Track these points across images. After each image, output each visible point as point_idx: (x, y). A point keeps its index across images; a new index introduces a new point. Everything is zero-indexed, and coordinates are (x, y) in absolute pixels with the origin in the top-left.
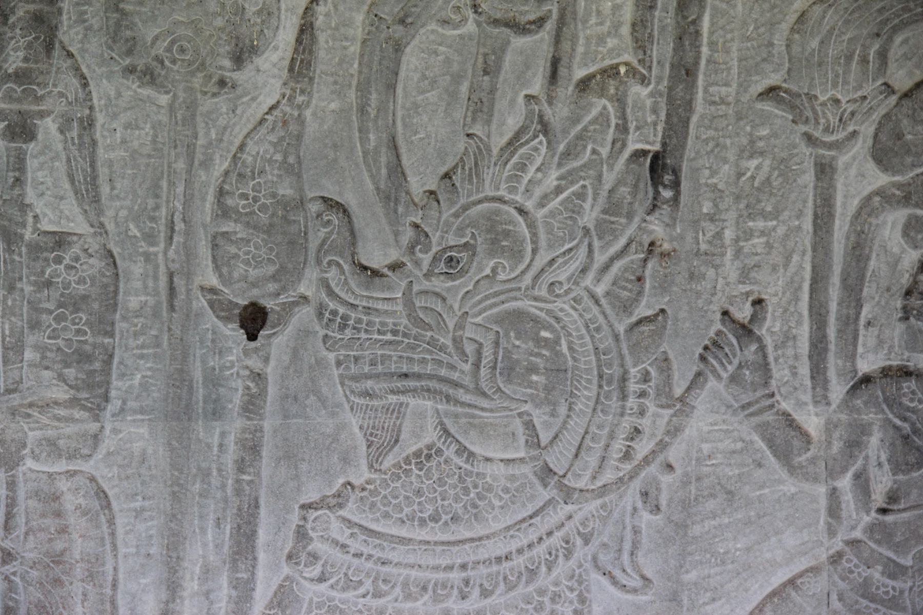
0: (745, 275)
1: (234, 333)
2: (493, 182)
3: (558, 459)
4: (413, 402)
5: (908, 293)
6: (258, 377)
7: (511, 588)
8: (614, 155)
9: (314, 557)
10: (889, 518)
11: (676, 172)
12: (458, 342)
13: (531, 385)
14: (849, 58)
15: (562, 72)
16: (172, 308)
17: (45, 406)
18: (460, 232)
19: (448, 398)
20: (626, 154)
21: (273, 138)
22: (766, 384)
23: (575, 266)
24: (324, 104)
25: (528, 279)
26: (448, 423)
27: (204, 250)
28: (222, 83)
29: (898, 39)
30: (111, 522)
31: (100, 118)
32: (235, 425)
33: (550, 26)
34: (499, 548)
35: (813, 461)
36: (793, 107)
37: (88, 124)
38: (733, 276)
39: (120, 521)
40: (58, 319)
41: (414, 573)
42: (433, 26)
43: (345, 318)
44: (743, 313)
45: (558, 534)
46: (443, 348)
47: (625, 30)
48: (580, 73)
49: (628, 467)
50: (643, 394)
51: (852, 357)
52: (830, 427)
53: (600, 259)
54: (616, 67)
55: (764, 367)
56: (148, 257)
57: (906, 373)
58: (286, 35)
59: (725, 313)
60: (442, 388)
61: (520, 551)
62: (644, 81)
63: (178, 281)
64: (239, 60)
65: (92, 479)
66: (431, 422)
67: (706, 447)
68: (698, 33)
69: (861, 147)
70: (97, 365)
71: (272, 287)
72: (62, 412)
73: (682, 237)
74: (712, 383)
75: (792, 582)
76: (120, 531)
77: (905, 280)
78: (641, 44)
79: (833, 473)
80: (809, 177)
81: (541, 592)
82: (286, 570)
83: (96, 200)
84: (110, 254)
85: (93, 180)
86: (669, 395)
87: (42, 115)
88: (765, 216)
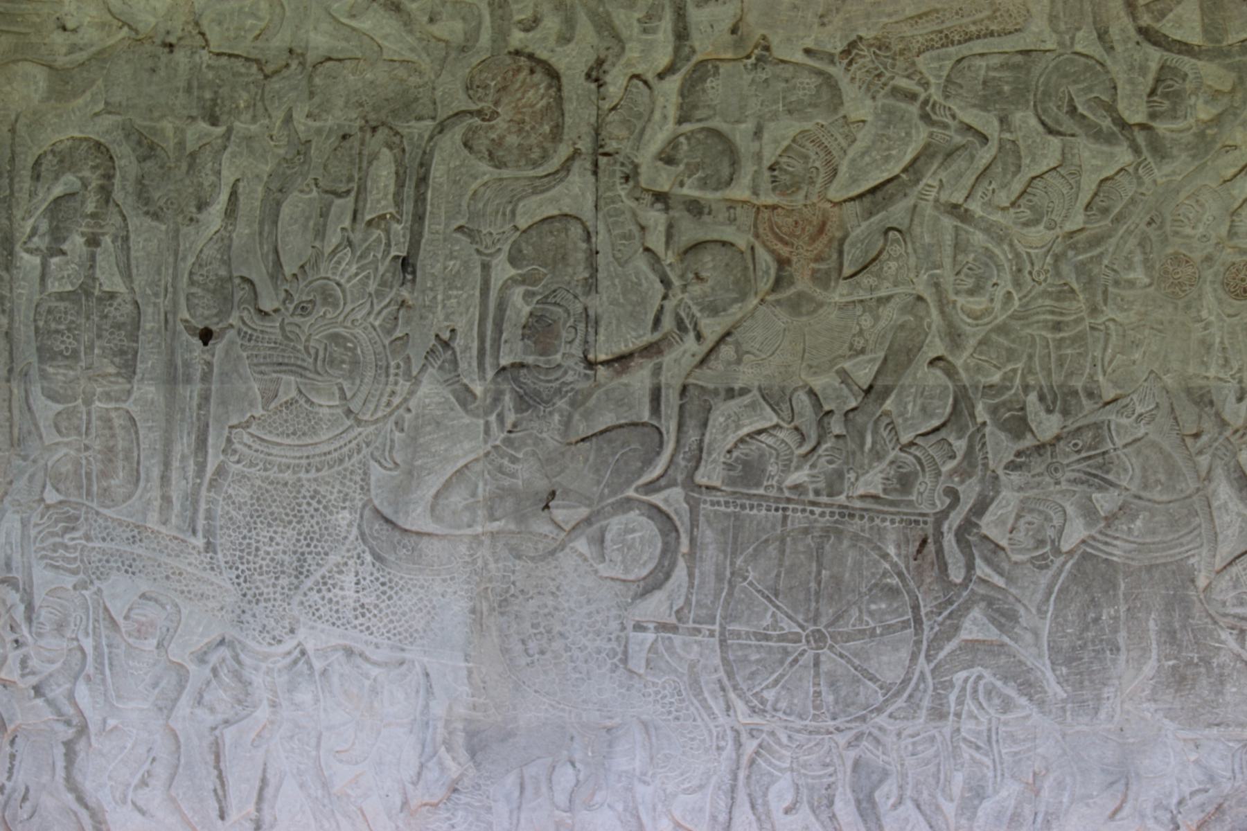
0: (447, 318)
1: (196, 342)
2: (325, 269)
3: (355, 406)
4: (285, 377)
5: (524, 327)
6: (209, 364)
7: (331, 467)
8: (384, 258)
9: (235, 451)
10: (513, 435)
11: (414, 266)
12: (306, 348)
13: (342, 369)
14: (497, 212)
15: (359, 216)
16: (166, 329)
17: (104, 376)
18: (308, 294)
19: (301, 375)
20: (390, 258)
21: (216, 247)
22: (456, 370)
23: (364, 311)
24: (242, 231)
25: (341, 318)
26: (302, 387)
27: (183, 301)
28: (191, 219)
29: (521, 205)
30: (137, 432)
31: (132, 236)
32: (198, 387)
33: (353, 194)
34: (325, 448)
35: (477, 408)
36: (470, 236)
37: (126, 239)
38: (442, 317)
39: (141, 432)
40: (112, 333)
41: (284, 460)
42: (296, 193)
43: (251, 335)
44: (446, 336)
45: (354, 442)
46: (299, 351)
47: (390, 197)
48: (368, 217)
49: (389, 410)
50: (396, 375)
51: (497, 358)
52: (486, 391)
53: (377, 308)
54: (385, 215)
55: (455, 362)
56: (155, 304)
57: (522, 365)
58: (224, 197)
59: (437, 336)
60: (299, 371)
61: (335, 450)
62: (399, 222)
63: (170, 317)
64: (200, 208)
65: (128, 412)
66: (293, 387)
67: (427, 401)
68: (425, 200)
69: (503, 256)
70: (130, 356)
71: (216, 320)
72: (113, 379)
73: (417, 299)
74: (430, 370)
75: (466, 466)
76: (141, 437)
77: (523, 321)
78: (398, 202)
79: (487, 413)
80: (478, 270)
81: (345, 470)
82: (222, 457)
83: (130, 276)
84: (136, 302)
85: (129, 266)
86: (410, 375)
87: (103, 234)
88: (457, 288)
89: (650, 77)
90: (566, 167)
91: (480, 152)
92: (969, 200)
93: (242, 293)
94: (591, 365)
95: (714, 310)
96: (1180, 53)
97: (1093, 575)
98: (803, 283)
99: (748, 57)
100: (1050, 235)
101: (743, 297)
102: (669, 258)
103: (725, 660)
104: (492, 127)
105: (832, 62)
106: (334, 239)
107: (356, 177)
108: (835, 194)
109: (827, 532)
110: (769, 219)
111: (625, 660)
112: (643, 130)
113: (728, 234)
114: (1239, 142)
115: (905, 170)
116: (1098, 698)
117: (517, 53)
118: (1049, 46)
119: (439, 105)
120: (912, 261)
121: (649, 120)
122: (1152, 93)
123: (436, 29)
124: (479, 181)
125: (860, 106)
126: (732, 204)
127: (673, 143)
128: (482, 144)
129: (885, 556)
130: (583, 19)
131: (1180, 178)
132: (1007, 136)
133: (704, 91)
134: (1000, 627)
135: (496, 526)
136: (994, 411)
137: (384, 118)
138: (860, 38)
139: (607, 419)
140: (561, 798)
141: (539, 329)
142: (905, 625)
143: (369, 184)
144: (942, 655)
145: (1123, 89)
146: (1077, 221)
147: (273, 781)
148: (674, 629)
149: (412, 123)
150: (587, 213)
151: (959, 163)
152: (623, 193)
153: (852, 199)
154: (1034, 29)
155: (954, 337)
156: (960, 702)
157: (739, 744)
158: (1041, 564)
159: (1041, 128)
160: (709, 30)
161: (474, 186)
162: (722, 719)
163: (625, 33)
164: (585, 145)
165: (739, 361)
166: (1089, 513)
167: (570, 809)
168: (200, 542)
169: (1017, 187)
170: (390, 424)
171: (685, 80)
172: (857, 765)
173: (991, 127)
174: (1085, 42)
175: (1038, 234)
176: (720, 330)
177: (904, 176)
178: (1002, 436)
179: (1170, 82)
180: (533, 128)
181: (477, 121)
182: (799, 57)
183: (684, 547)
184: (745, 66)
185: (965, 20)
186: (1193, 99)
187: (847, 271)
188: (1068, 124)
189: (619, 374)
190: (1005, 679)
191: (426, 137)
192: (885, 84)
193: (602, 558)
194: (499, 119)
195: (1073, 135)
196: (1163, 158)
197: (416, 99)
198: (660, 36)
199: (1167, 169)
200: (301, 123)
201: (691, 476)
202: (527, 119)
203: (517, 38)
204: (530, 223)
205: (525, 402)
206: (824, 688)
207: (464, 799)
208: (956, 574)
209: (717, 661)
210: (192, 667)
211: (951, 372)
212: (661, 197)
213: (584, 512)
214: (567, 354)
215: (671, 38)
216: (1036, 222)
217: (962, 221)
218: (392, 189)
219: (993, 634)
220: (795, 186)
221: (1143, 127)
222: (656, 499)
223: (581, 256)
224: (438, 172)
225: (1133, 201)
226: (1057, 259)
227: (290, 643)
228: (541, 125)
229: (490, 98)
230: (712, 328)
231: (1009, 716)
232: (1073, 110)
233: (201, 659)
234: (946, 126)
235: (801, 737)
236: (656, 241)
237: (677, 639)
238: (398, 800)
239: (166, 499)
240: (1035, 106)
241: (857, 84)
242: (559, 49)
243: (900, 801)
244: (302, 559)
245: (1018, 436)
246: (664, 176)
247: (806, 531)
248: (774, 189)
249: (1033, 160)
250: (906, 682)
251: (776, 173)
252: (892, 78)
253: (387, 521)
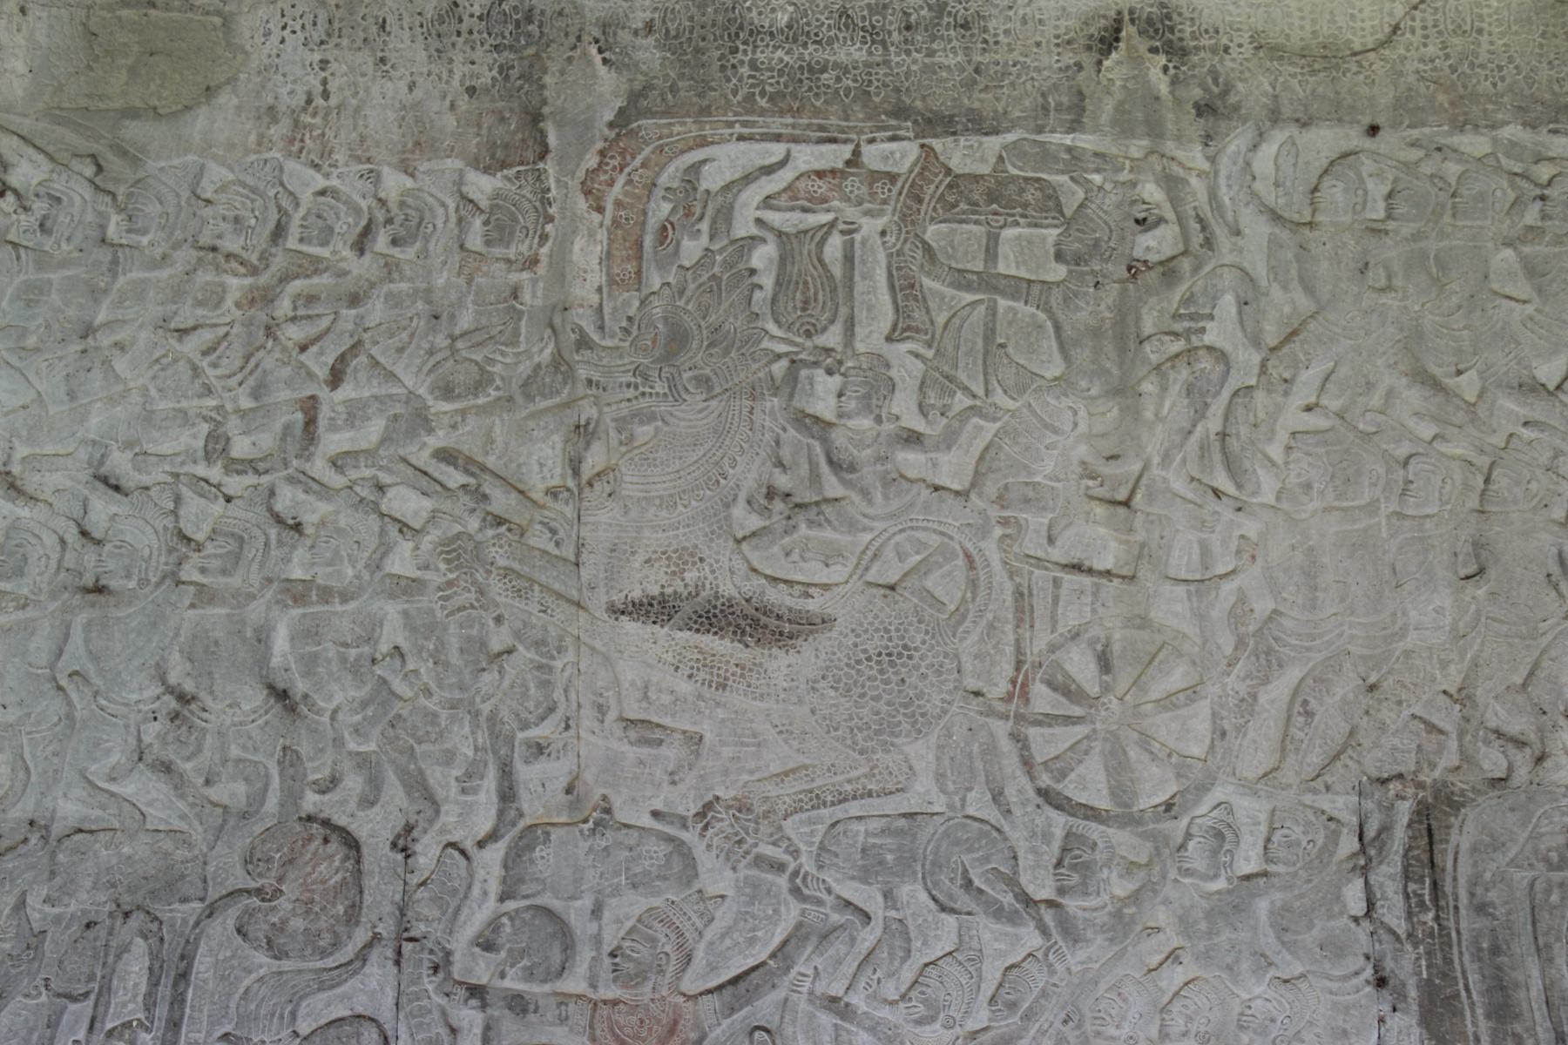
14: (273, 1015)
15: (97, 1025)
29: (304, 1004)
33: (93, 997)
42: (20, 998)
47: (140, 999)
48: (109, 1026)
54: (131, 1022)
62: (148, 1030)
68: (183, 1001)
78: (149, 1006)
89: (469, 845)
90: (362, 957)
91: (257, 939)
92: (851, 992)
96: (1086, 818)
99: (585, 821)
104: (273, 909)
105: (685, 827)
107: (99, 975)
108: (690, 984)
110: (609, 1018)
112: (458, 910)
114: (1162, 924)
115: (773, 956)
117: (310, 819)
118: (936, 809)
119: (210, 883)
121: (466, 897)
122: (1059, 864)
123: (213, 793)
124: (254, 976)
125: (717, 877)
126: (563, 999)
127: (494, 925)
128: (259, 929)
130: (391, 777)
131: (1097, 966)
132: (893, 914)
133: (532, 861)
137: (134, 906)
138: (717, 798)
143: (115, 982)
145: (1025, 860)
146: (981, 1018)
149: (176, 906)
150: (386, 1014)
151: (838, 947)
152: (430, 988)
153: (710, 992)
154: (919, 787)
159: (932, 905)
160: (540, 789)
161: (246, 983)
163: (440, 794)
164: (386, 929)
169: (908, 975)
171: (509, 847)
174: (978, 803)
177: (771, 962)
179: (1077, 852)
180: (323, 909)
181: (255, 901)
182: (647, 821)
184: (581, 831)
185: (840, 778)
186: (1106, 871)
188: (964, 901)
191: (191, 923)
192: (747, 853)
194: (282, 899)
195: (969, 914)
196: (1076, 941)
197: (183, 877)
198: (482, 797)
199: (1081, 955)
200: (36, 909)
202: (317, 898)
203: (311, 801)
204: (314, 1026)
212: (476, 992)
215: (495, 799)
216: (930, 1019)
217: (842, 1019)
218: (143, 989)
220: (639, 977)
221: (1050, 903)
224: (203, 966)
225: (1044, 994)
228: (334, 904)
229: (273, 874)
232: (968, 884)
234: (820, 902)
240: (924, 878)
241: (714, 853)
242: (361, 814)
246: (482, 965)
248: (615, 981)
249: (925, 943)
251: (617, 960)
252: (756, 845)
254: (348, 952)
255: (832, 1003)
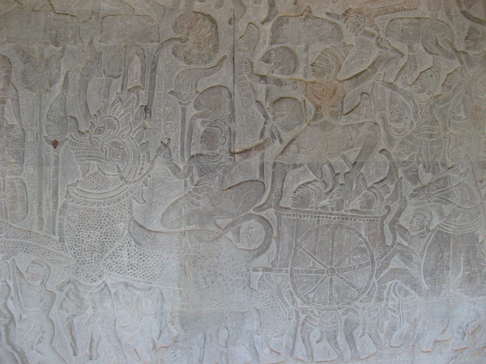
0: (166, 134)
3: (125, 174)
4: (92, 162)
5: (202, 137)
6: (57, 157)
7: (115, 203)
8: (137, 106)
9: (70, 197)
10: (197, 187)
11: (150, 110)
12: (101, 149)
13: (118, 158)
14: (189, 85)
15: (124, 87)
16: (37, 141)
17: (10, 163)
18: (102, 124)
19: (100, 161)
20: (139, 106)
21: (59, 103)
22: (171, 158)
23: (128, 131)
25: (117, 134)
26: (100, 167)
27: (44, 128)
28: (47, 90)
29: (199, 81)
30: (26, 189)
31: (20, 99)
32: (53, 167)
33: (121, 77)
34: (111, 194)
35: (181, 174)
36: (176, 96)
37: (18, 100)
38: (163, 133)
39: (28, 189)
40: (12, 144)
41: (93, 200)
42: (95, 77)
43: (76, 143)
44: (166, 142)
45: (125, 191)
46: (98, 150)
47: (139, 78)
48: (129, 88)
49: (140, 176)
50: (143, 160)
51: (190, 152)
52: (185, 167)
53: (134, 130)
55: (170, 154)
56: (32, 130)
58: (62, 79)
59: (162, 142)
61: (116, 195)
62: (143, 89)
63: (38, 135)
64: (51, 85)
65: (21, 180)
66: (96, 166)
67: (158, 172)
68: (155, 79)
69: (192, 105)
70: (21, 154)
71: (59, 136)
72: (14, 165)
73: (152, 125)
74: (159, 157)
75: (176, 201)
76: (28, 191)
77: (201, 134)
79: (185, 177)
80: (180, 111)
81: (121, 204)
82: (65, 199)
83: (20, 117)
84: (23, 129)
85: (19, 112)
86: (150, 160)
87: (7, 98)
88: (170, 120)
89: (258, 23)
91: (180, 57)
92: (396, 81)
93: (71, 123)
94: (233, 154)
95: (288, 129)
96: (477, 22)
97: (442, 240)
98: (327, 117)
99: (302, 15)
100: (428, 97)
101: (300, 123)
102: (267, 105)
103: (292, 283)
104: (186, 45)
105: (338, 18)
106: (113, 98)
107: (123, 69)
108: (340, 77)
109: (336, 226)
110: (312, 88)
111: (249, 285)
112: (255, 48)
113: (293, 94)
115: (370, 67)
116: (441, 288)
118: (427, 17)
119: (161, 36)
120: (373, 107)
121: (258, 43)
122: (467, 38)
124: (180, 70)
125: (350, 38)
126: (295, 81)
127: (268, 53)
129: (360, 235)
131: (477, 74)
132: (411, 54)
133: (282, 30)
134: (406, 263)
135: (191, 227)
136: (406, 172)
138: (350, 9)
139: (240, 179)
140: (222, 343)
141: (209, 138)
142: (368, 264)
143: (129, 72)
144: (382, 275)
147: (96, 340)
148: (271, 270)
149: (149, 44)
150: (230, 85)
152: (246, 76)
153: (348, 80)
154: (421, 9)
155: (390, 140)
156: (388, 294)
157: (298, 317)
158: (422, 236)
159: (424, 51)
160: (284, 3)
161: (177, 73)
162: (291, 307)
165: (299, 152)
166: (441, 214)
167: (226, 346)
168: (57, 238)
169: (415, 76)
170: (141, 183)
171: (273, 24)
172: (346, 321)
173: (405, 50)
174: (441, 15)
175: (424, 97)
176: (290, 138)
177: (369, 70)
178: (408, 183)
179: (473, 35)
180: (205, 46)
181: (179, 43)
182: (324, 16)
183: (275, 234)
184: (300, 19)
185: (394, 3)
186: (482, 42)
187: (345, 112)
188: (436, 50)
189: (245, 158)
190: (406, 284)
191: (155, 50)
192: (361, 30)
193: (239, 241)
194: (189, 42)
195: (437, 55)
196: (471, 66)
197: (150, 33)
200: (97, 44)
201: (278, 203)
202: (202, 42)
204: (204, 89)
205: (202, 172)
206: (334, 292)
207: (180, 344)
208: (389, 242)
209: (289, 283)
210: (57, 292)
211: (388, 156)
212: (263, 78)
213: (230, 220)
214: (222, 149)
215: (267, 6)
216: (423, 91)
217: (393, 90)
218: (140, 74)
219: (402, 265)
221: (463, 52)
222: (263, 214)
223: (227, 104)
224: (161, 66)
225: (460, 84)
226: (431, 107)
227: (100, 282)
228: (208, 44)
229: (185, 32)
230: (287, 137)
231: (407, 298)
232: (437, 44)
233: (61, 289)
234: (386, 49)
235: (324, 312)
236: (262, 97)
237: (272, 275)
238: (151, 346)
239: (41, 219)
240: (422, 41)
241: (349, 29)
242: (216, 10)
243: (363, 334)
244: (103, 244)
245: (415, 183)
246: (264, 68)
247: (327, 226)
248: (313, 75)
249: (421, 65)
250: (367, 287)
251: (314, 67)
252: (364, 27)
253: (141, 226)
254: (214, 62)
255: (390, 85)
